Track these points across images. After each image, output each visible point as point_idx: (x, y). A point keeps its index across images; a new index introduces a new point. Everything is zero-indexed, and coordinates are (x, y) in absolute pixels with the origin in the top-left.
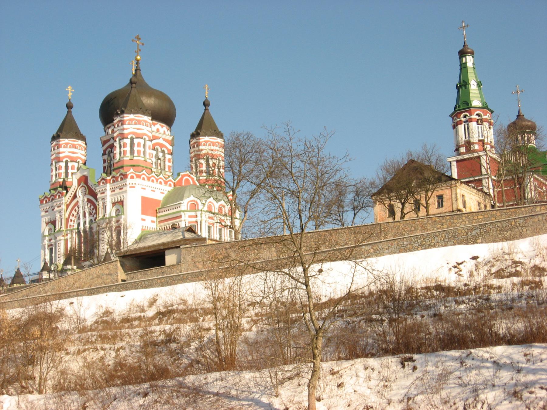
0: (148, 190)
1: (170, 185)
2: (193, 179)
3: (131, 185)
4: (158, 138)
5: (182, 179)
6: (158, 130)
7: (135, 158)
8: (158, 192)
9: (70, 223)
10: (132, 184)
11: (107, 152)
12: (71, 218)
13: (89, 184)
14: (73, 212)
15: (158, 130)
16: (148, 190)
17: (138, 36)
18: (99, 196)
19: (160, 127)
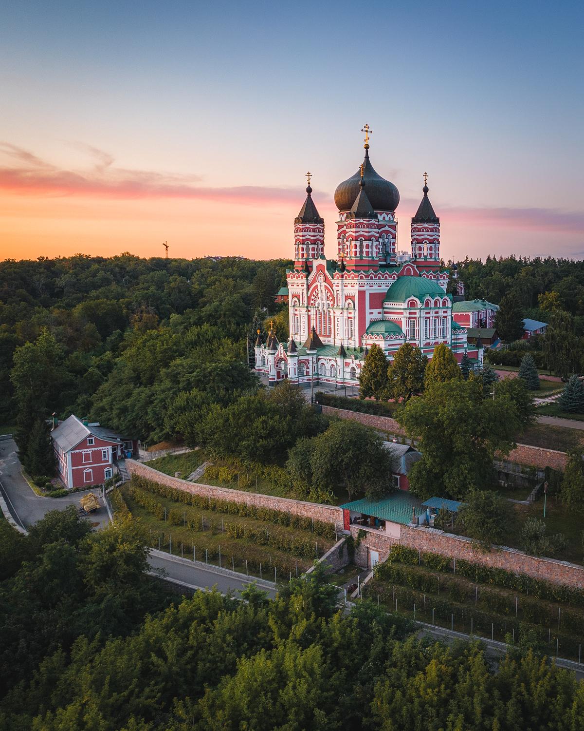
0: (376, 287)
1: (394, 278)
2: (413, 267)
4: (385, 226)
5: (404, 269)
6: (384, 218)
7: (364, 258)
8: (383, 287)
9: (312, 302)
12: (313, 297)
14: (314, 293)
15: (384, 218)
16: (376, 287)
17: (367, 125)
18: (335, 288)
19: (386, 216)
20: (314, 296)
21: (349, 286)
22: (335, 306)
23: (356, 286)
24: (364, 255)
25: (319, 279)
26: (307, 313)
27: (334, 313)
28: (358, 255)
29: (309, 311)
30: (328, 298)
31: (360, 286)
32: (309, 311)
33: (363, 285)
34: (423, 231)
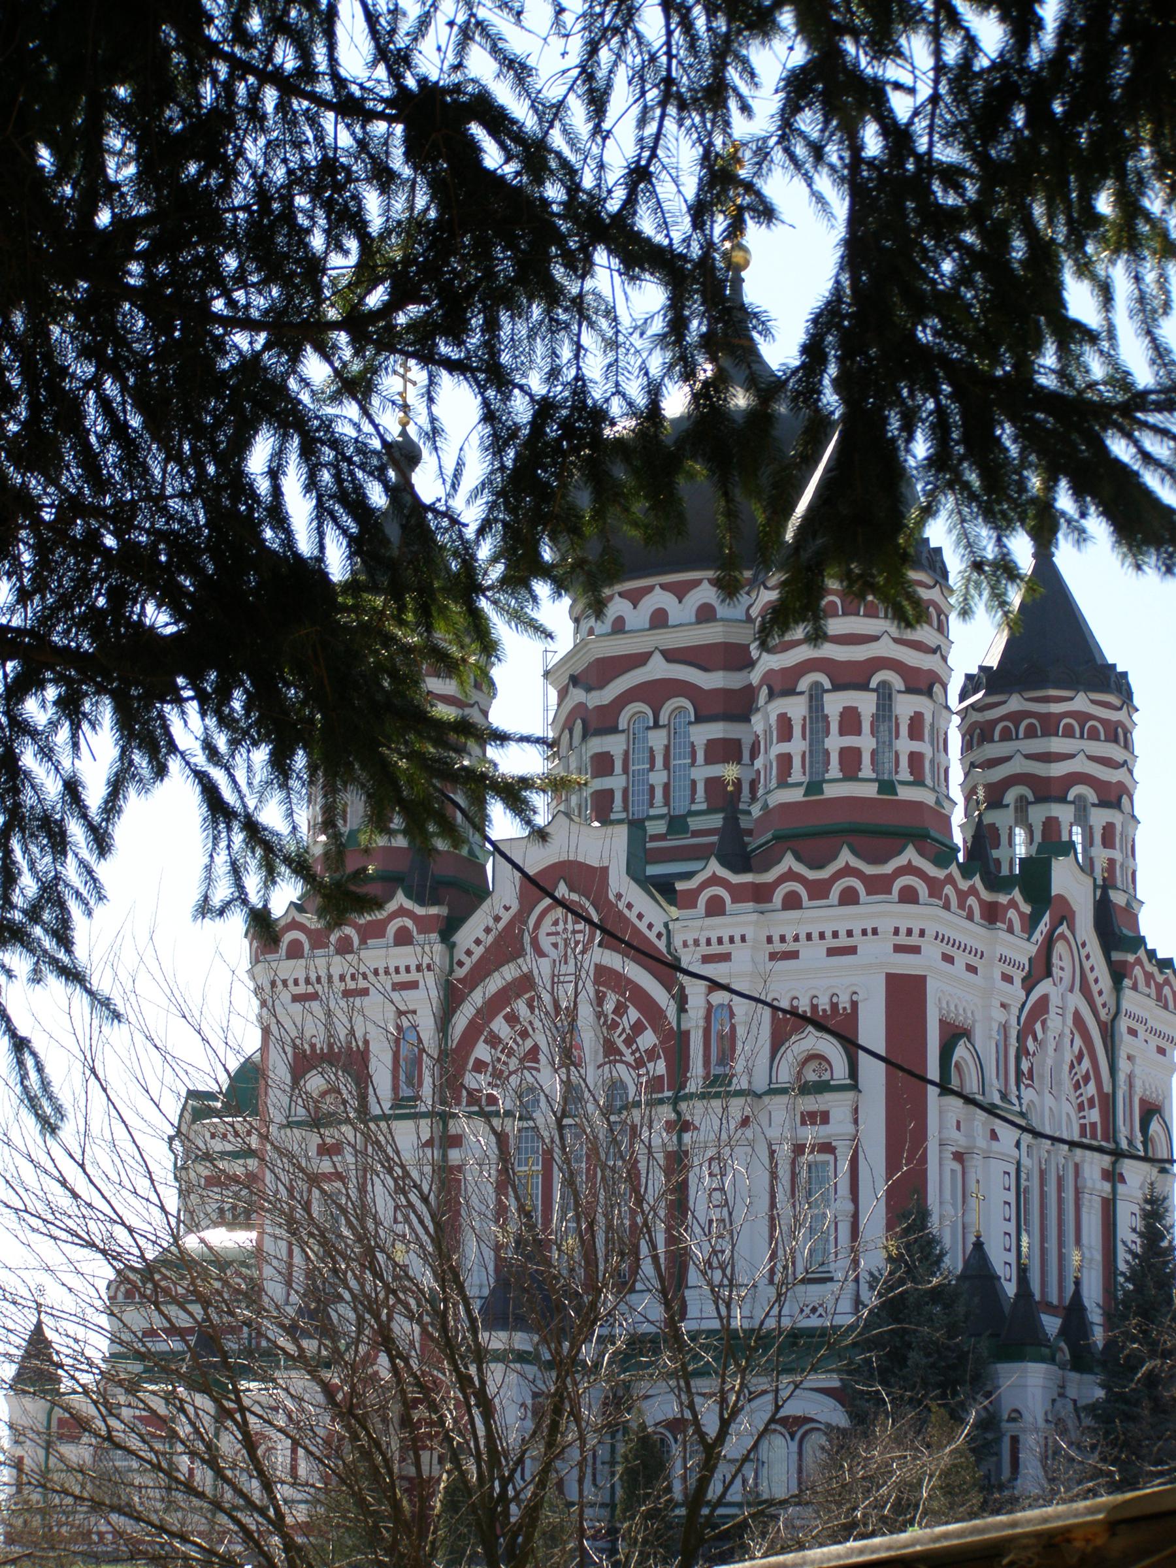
3: (903, 939)
10: (909, 932)
11: (623, 724)
12: (482, 1051)
13: (612, 897)
14: (499, 1026)
20: (494, 1041)
21: (812, 953)
22: (692, 1087)
23: (866, 946)
24: (905, 774)
25: (545, 943)
26: (435, 1154)
27: (681, 1126)
28: (866, 771)
29: (456, 1141)
30: (610, 1049)
31: (898, 949)
32: (456, 1141)
33: (914, 940)
34: (1069, 733)
